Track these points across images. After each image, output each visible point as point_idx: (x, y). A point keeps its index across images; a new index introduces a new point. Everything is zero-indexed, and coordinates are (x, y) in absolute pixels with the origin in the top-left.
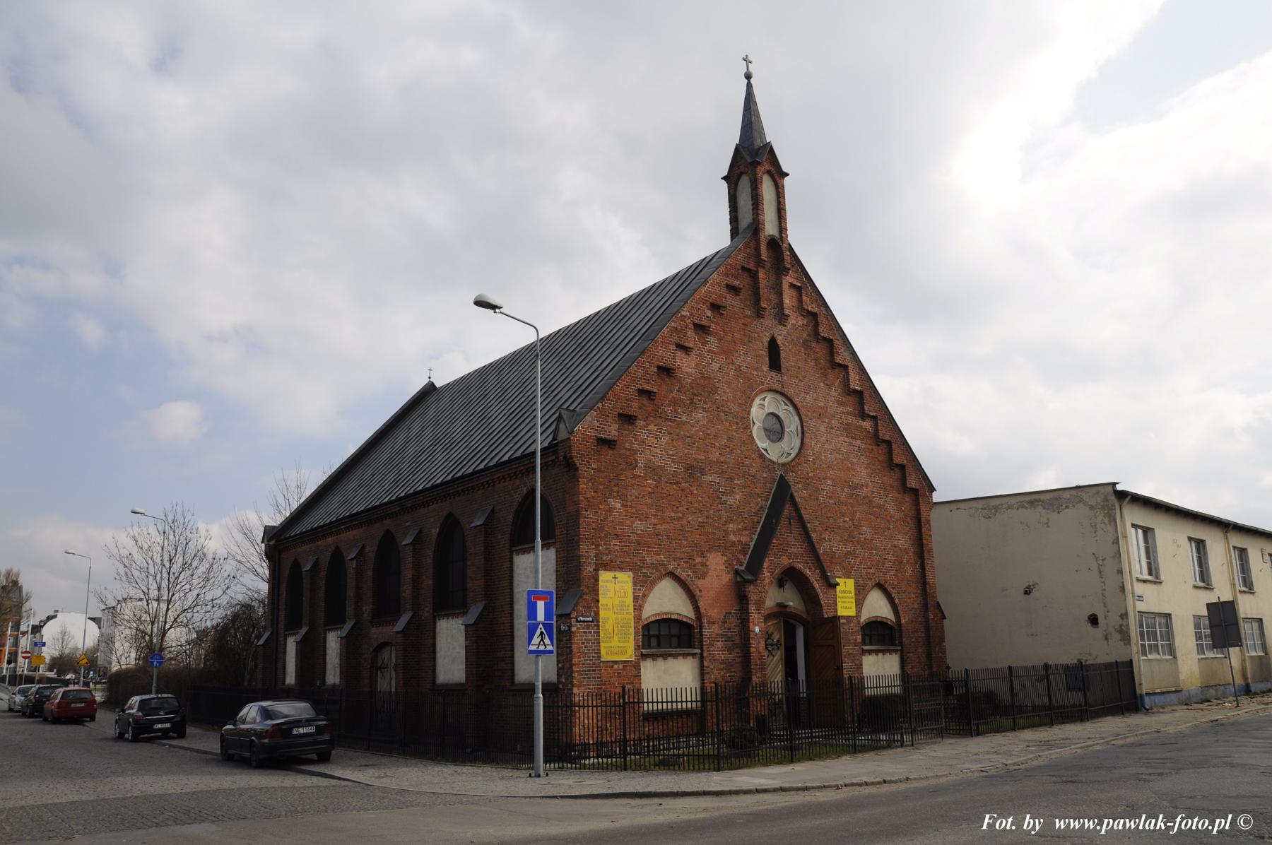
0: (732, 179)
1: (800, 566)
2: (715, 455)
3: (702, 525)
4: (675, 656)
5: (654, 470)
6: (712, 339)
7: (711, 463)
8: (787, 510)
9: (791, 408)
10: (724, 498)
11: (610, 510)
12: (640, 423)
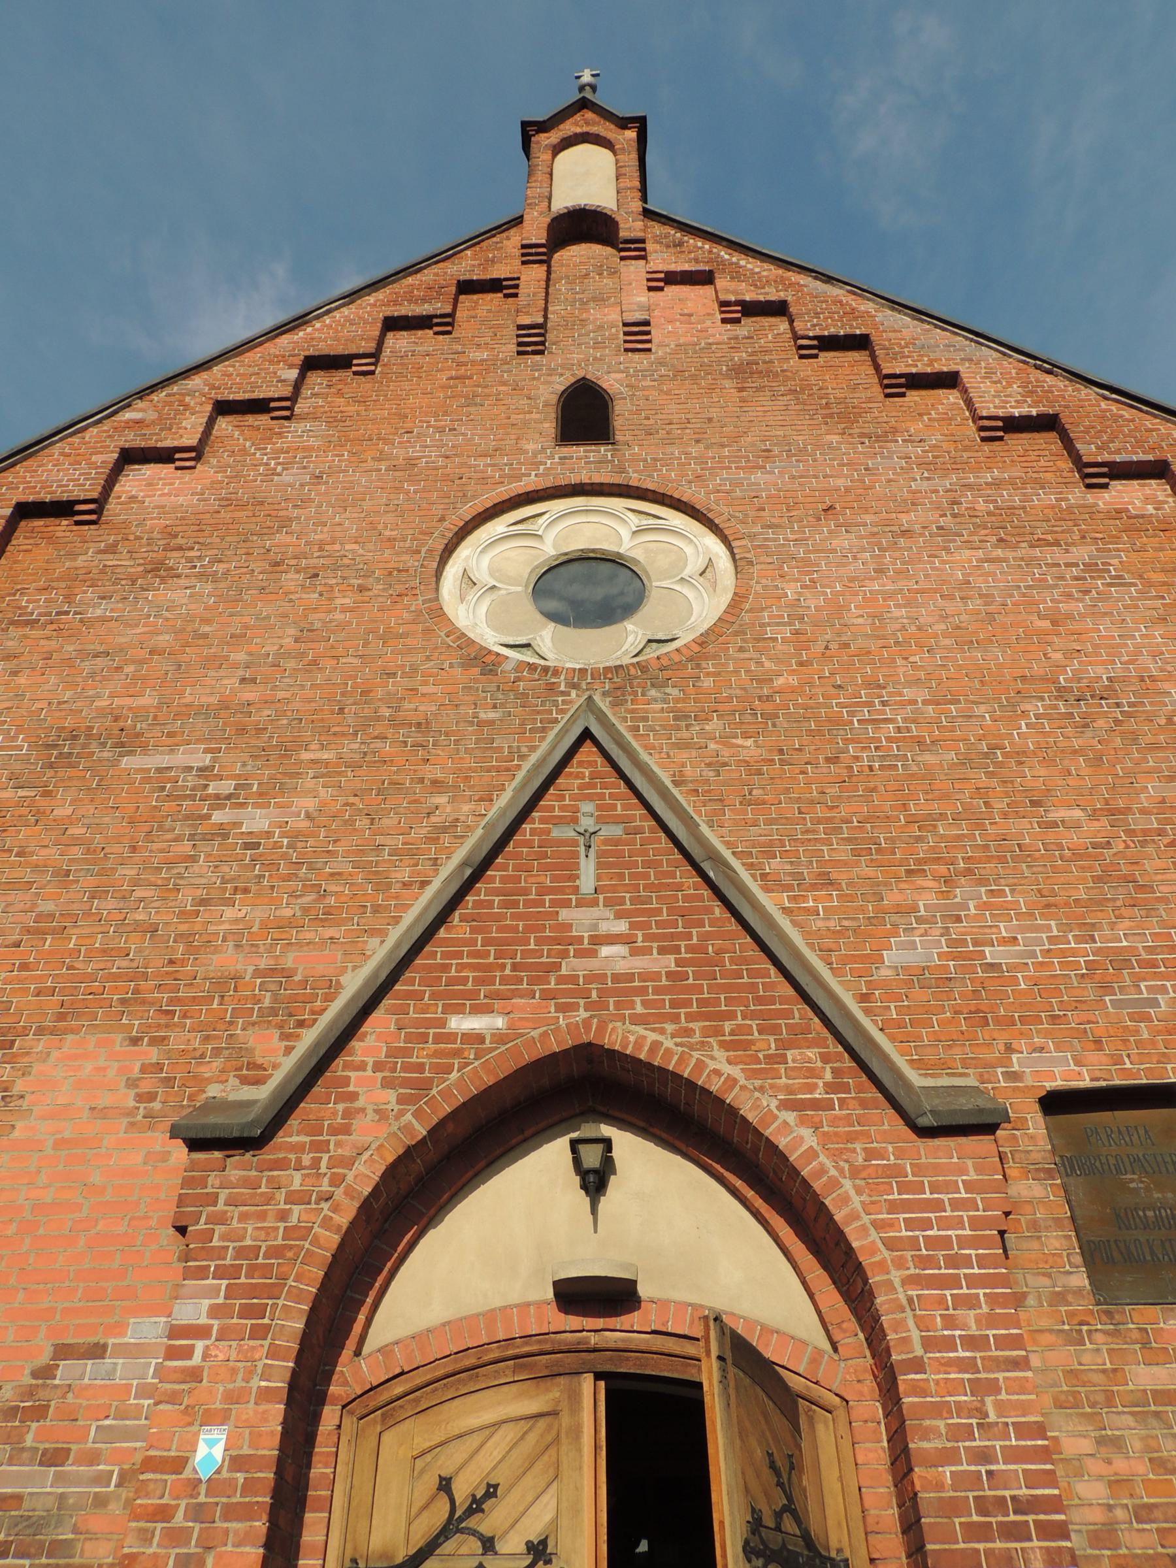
1: (630, 1036)
8: (585, 810)
10: (218, 817)
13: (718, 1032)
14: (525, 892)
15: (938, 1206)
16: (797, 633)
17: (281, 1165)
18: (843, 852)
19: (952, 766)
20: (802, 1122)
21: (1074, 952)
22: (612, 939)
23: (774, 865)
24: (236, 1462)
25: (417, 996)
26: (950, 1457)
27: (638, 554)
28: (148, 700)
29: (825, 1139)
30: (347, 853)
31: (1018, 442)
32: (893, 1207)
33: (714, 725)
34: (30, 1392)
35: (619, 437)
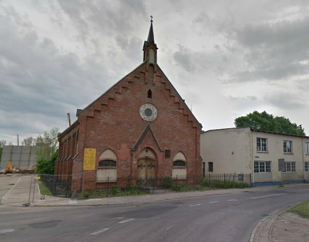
0: (144, 49)
1: (150, 147)
3: (121, 137)
4: (109, 169)
5: (105, 123)
6: (129, 91)
8: (149, 132)
9: (154, 107)
12: (102, 112)
31: (176, 104)
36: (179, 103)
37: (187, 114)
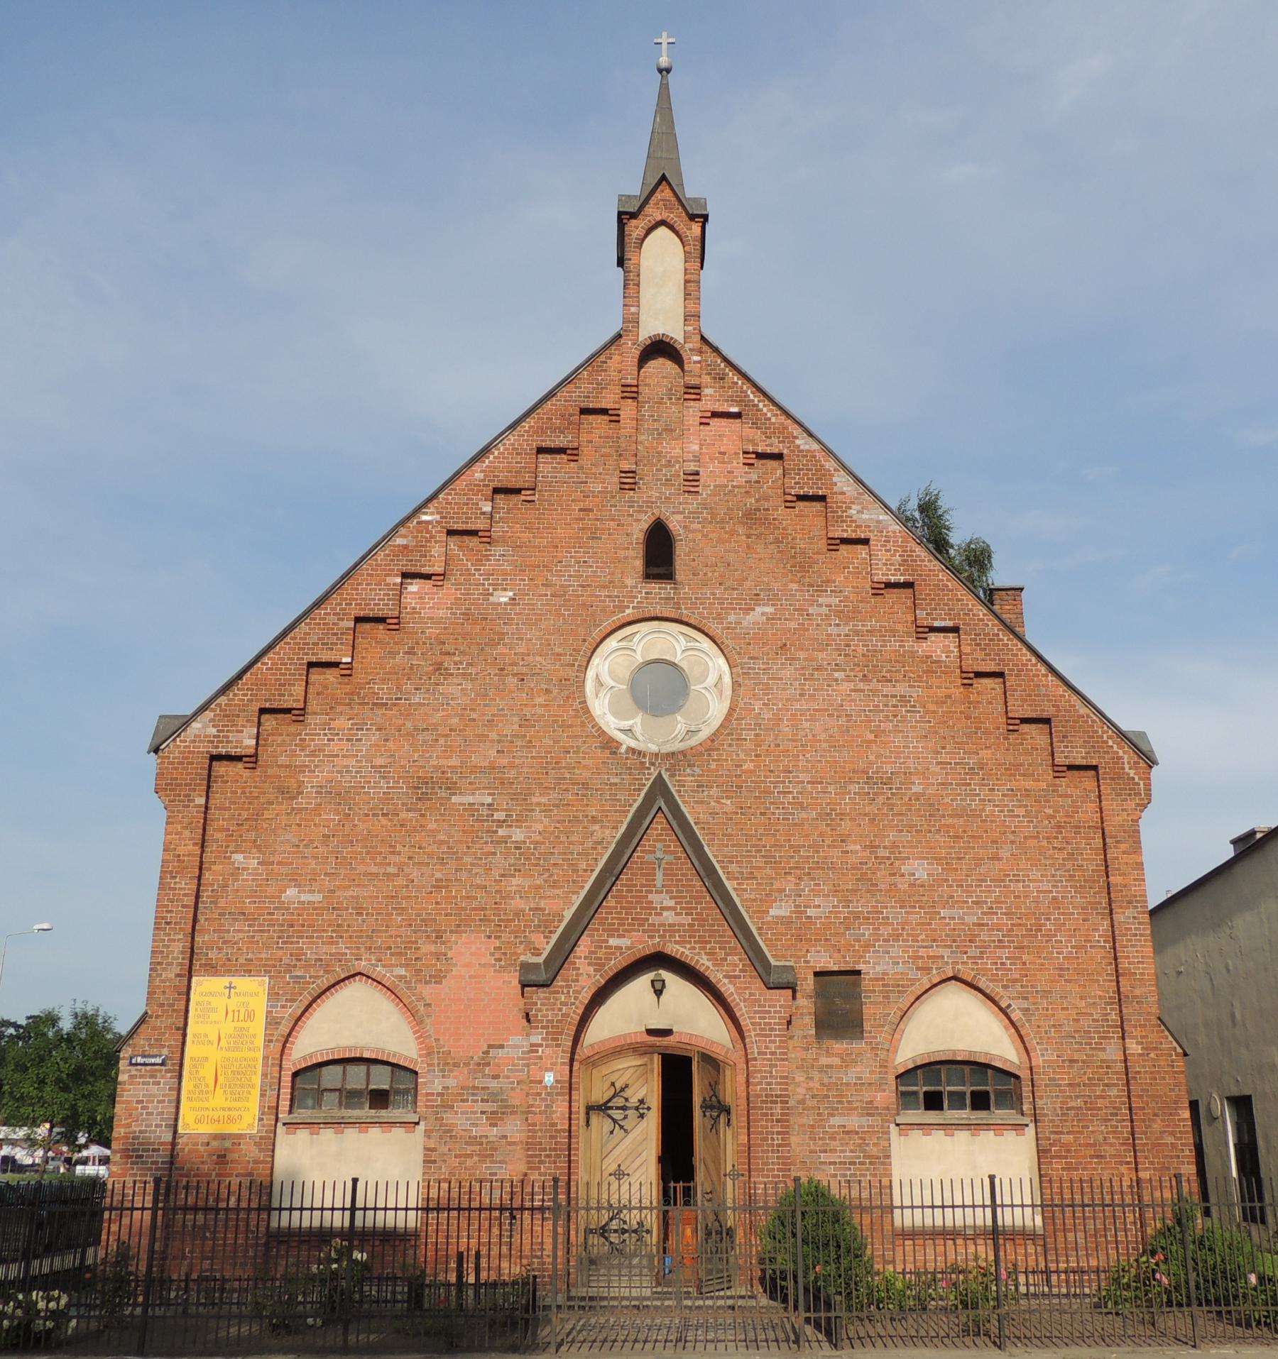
1: (673, 949)
2: (486, 755)
5: (336, 795)
6: (498, 550)
7: (474, 769)
8: (659, 845)
9: (706, 644)
10: (501, 832)
11: (236, 872)
13: (704, 948)
14: (635, 886)
15: (769, 1012)
16: (756, 735)
17: (558, 992)
18: (759, 861)
19: (813, 819)
20: (730, 982)
21: (840, 912)
22: (668, 909)
23: (733, 868)
24: (557, 1082)
25: (598, 930)
26: (760, 1083)
27: (684, 665)
28: (455, 761)
29: (737, 988)
30: (559, 854)
31: (893, 596)
32: (756, 1012)
33: (714, 791)
34: (483, 1059)
35: (679, 576)
36: (909, 585)
37: (991, 667)
